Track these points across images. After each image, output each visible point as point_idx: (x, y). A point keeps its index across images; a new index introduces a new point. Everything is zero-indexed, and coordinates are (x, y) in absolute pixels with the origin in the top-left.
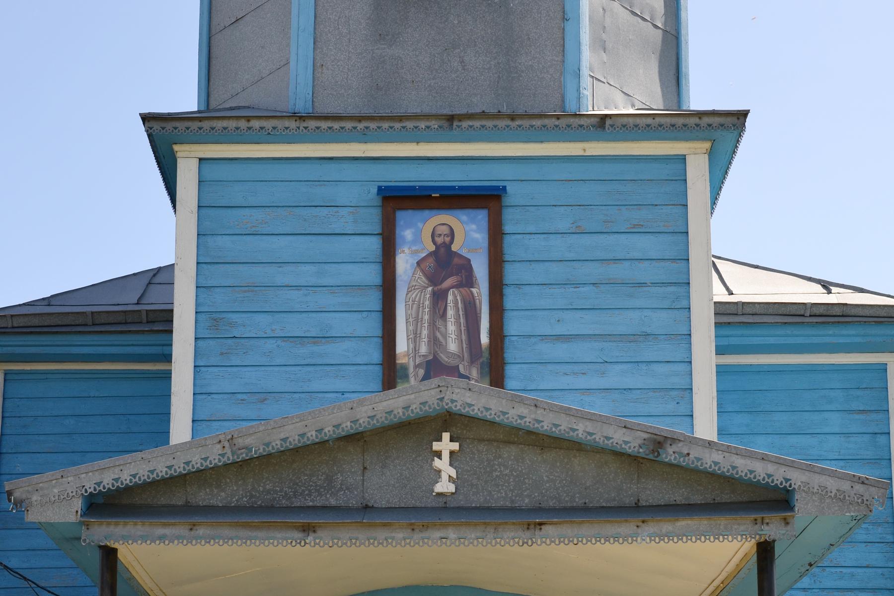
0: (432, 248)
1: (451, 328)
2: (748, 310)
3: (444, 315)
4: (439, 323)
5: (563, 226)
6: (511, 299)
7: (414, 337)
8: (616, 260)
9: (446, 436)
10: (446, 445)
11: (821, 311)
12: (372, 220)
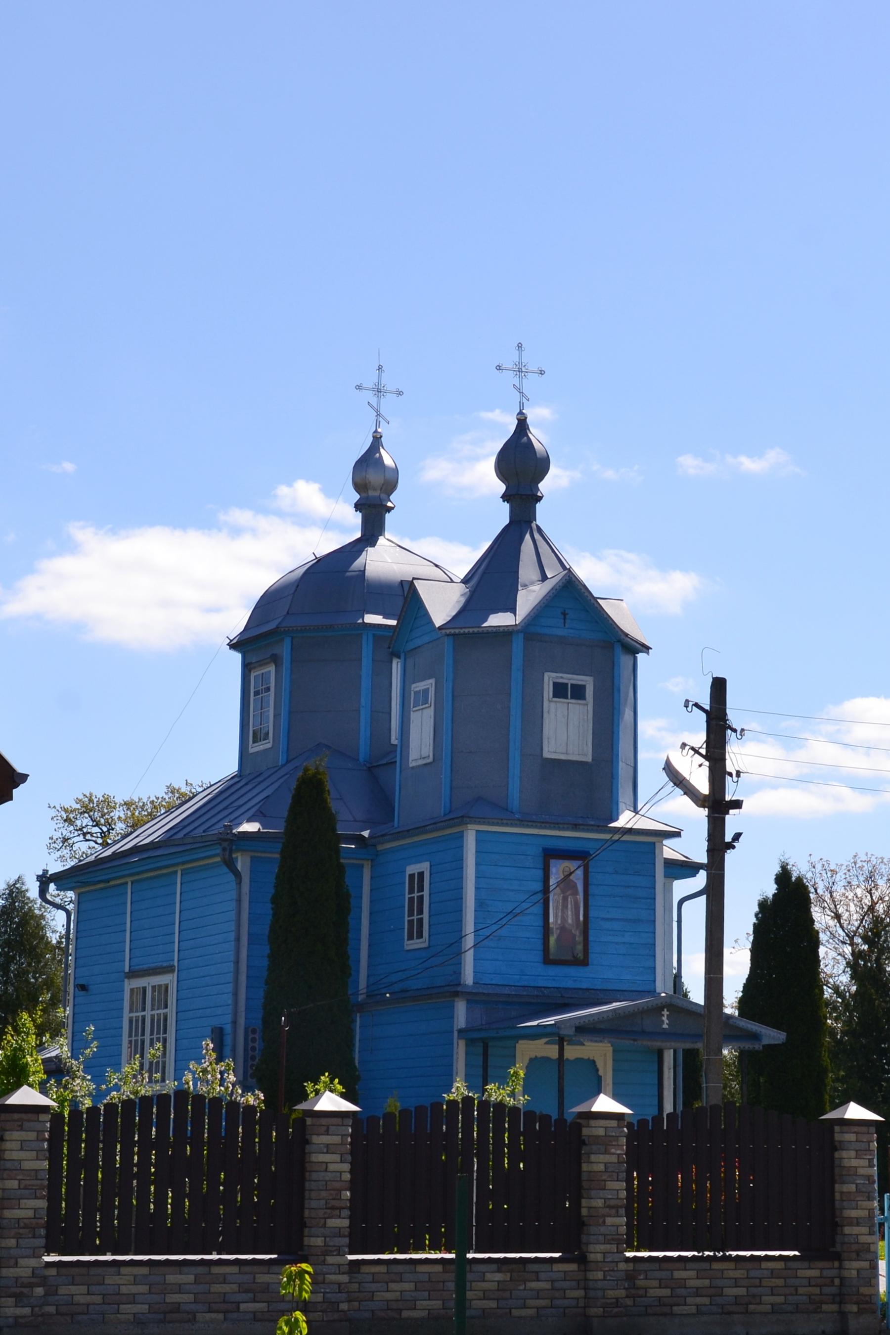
1: (570, 913)
7: (556, 916)
8: (629, 887)
9: (665, 1010)
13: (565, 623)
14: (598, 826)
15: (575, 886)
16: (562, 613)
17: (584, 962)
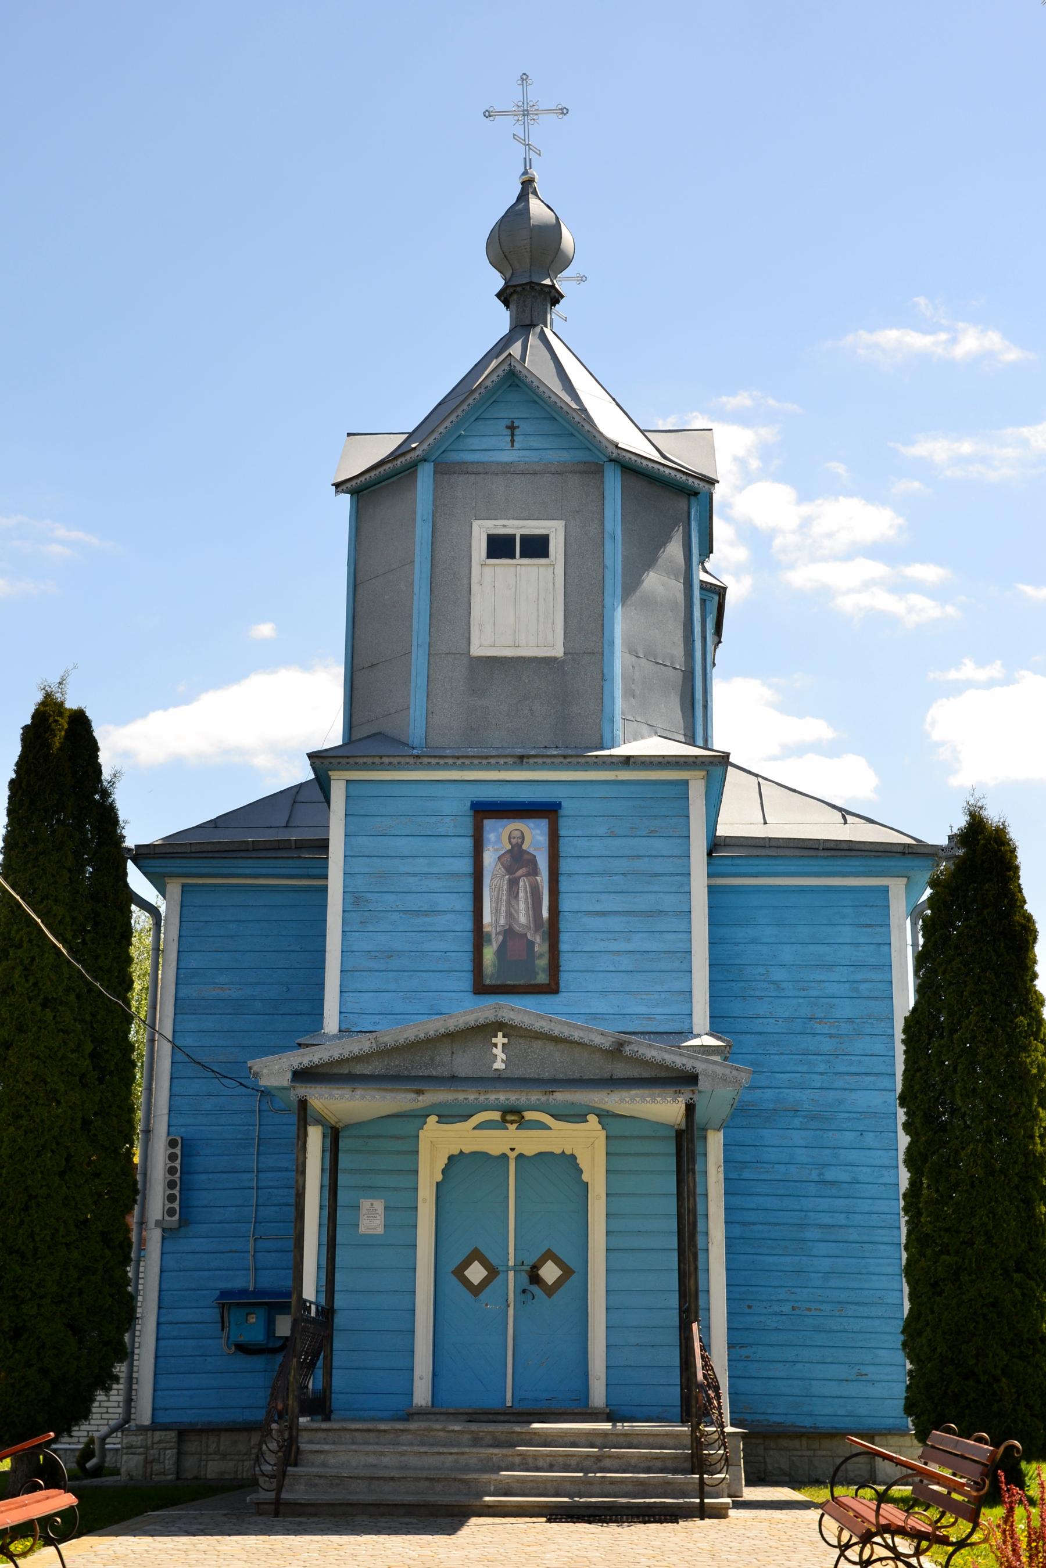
0: (509, 847)
1: (522, 905)
2: (773, 844)
3: (517, 896)
4: (513, 902)
5: (602, 831)
6: (564, 885)
7: (496, 912)
8: (639, 857)
9: (500, 1034)
10: (500, 1040)
11: (832, 845)
12: (468, 822)
13: (513, 441)
14: (565, 757)
15: (533, 862)
16: (508, 427)
17: (552, 988)
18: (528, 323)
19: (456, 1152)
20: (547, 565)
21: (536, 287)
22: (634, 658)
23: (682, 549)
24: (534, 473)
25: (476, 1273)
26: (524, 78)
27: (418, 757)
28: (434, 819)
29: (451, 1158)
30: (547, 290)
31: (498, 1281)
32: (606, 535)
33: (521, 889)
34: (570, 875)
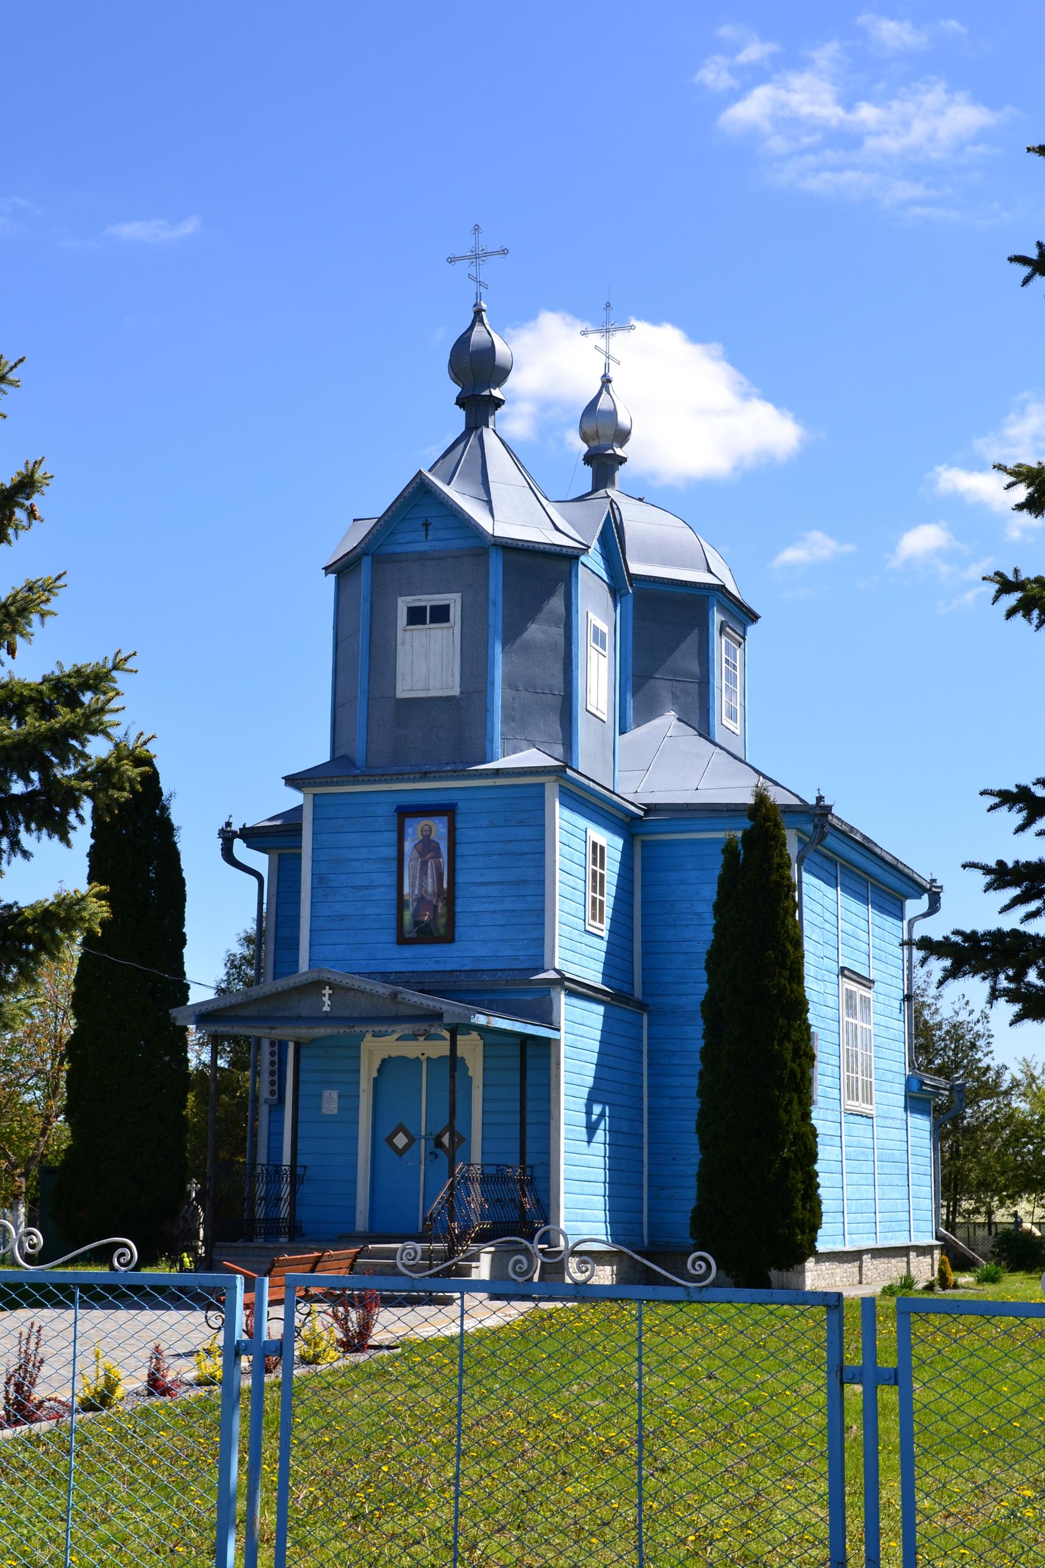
0: (421, 838)
1: (430, 880)
2: (691, 808)
3: (426, 874)
4: (424, 877)
5: (484, 823)
6: (459, 863)
7: (412, 886)
8: (510, 841)
9: (327, 987)
10: (327, 991)
11: (733, 807)
12: (394, 820)
13: (427, 535)
14: (455, 771)
15: (437, 848)
16: (423, 525)
17: (449, 938)
18: (473, 426)
19: (386, 1057)
20: (448, 628)
21: (478, 398)
22: (514, 692)
23: (563, 602)
24: (440, 559)
25: (401, 1140)
26: (477, 228)
27: (356, 776)
28: (372, 819)
29: (384, 1061)
30: (487, 398)
31: (414, 1147)
32: (490, 602)
33: (429, 868)
34: (463, 856)
